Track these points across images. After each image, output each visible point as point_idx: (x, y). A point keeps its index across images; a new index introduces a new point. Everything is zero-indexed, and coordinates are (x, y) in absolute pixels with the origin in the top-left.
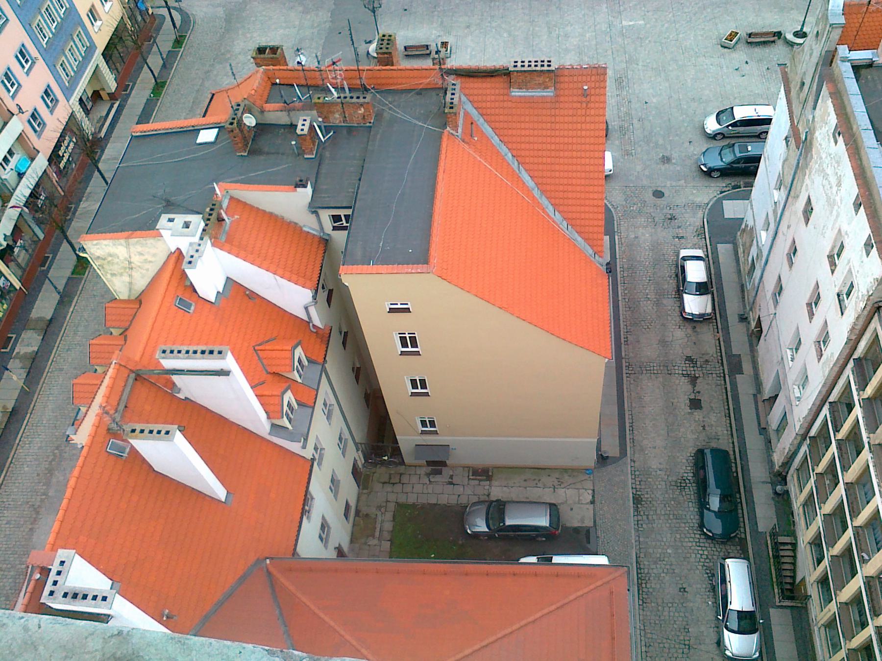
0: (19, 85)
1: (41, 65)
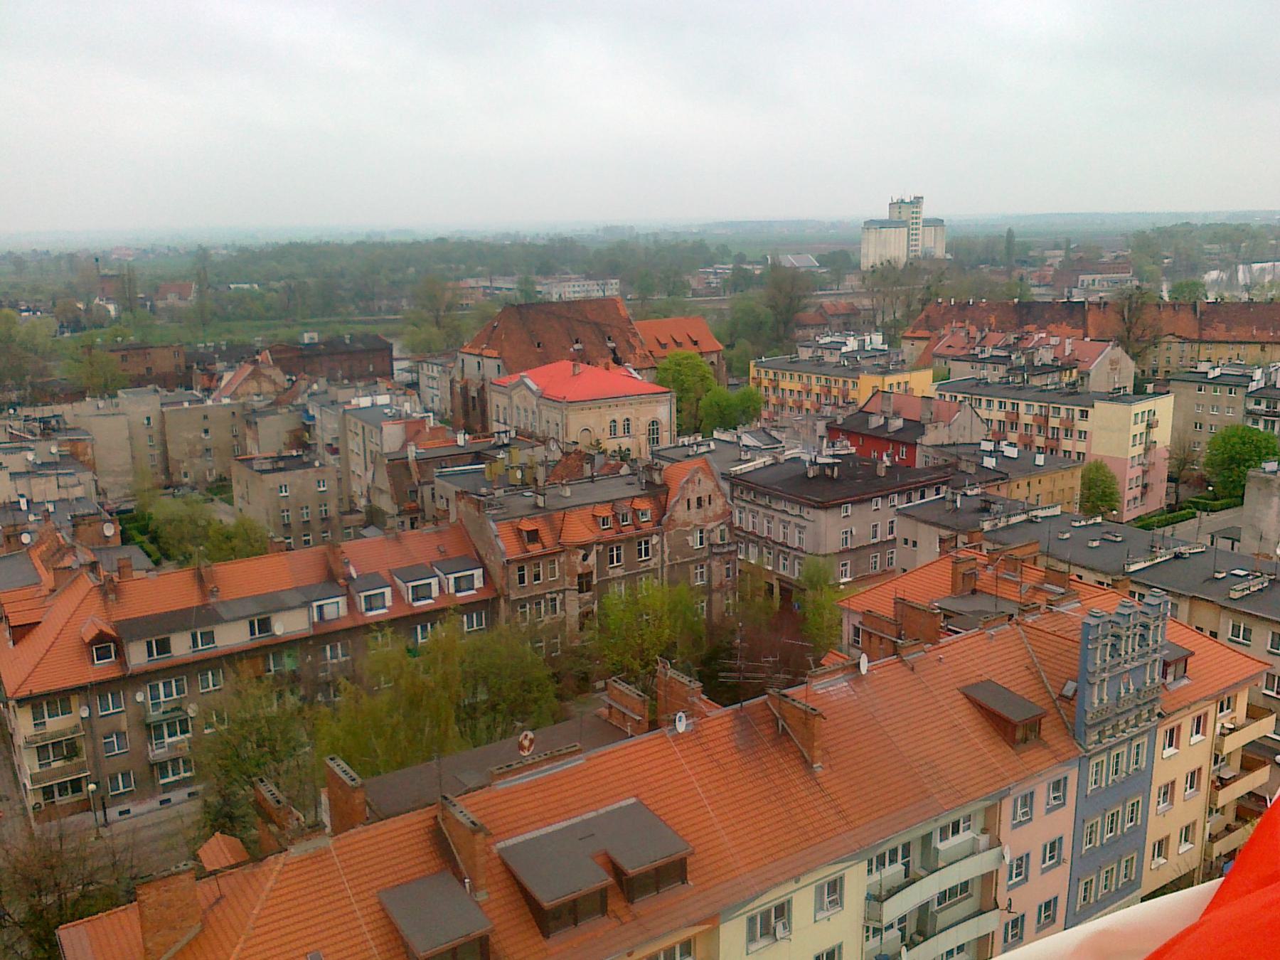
0: (1026, 878)
1: (1063, 871)
